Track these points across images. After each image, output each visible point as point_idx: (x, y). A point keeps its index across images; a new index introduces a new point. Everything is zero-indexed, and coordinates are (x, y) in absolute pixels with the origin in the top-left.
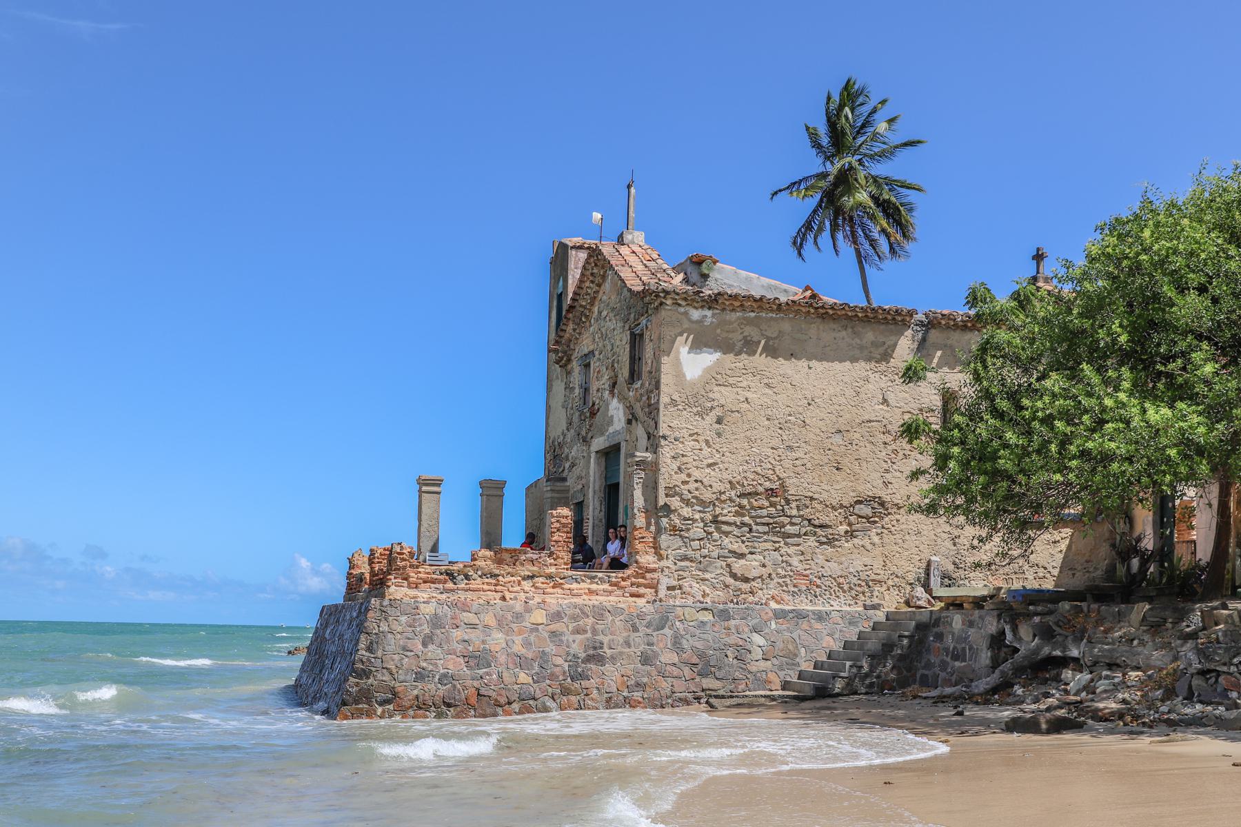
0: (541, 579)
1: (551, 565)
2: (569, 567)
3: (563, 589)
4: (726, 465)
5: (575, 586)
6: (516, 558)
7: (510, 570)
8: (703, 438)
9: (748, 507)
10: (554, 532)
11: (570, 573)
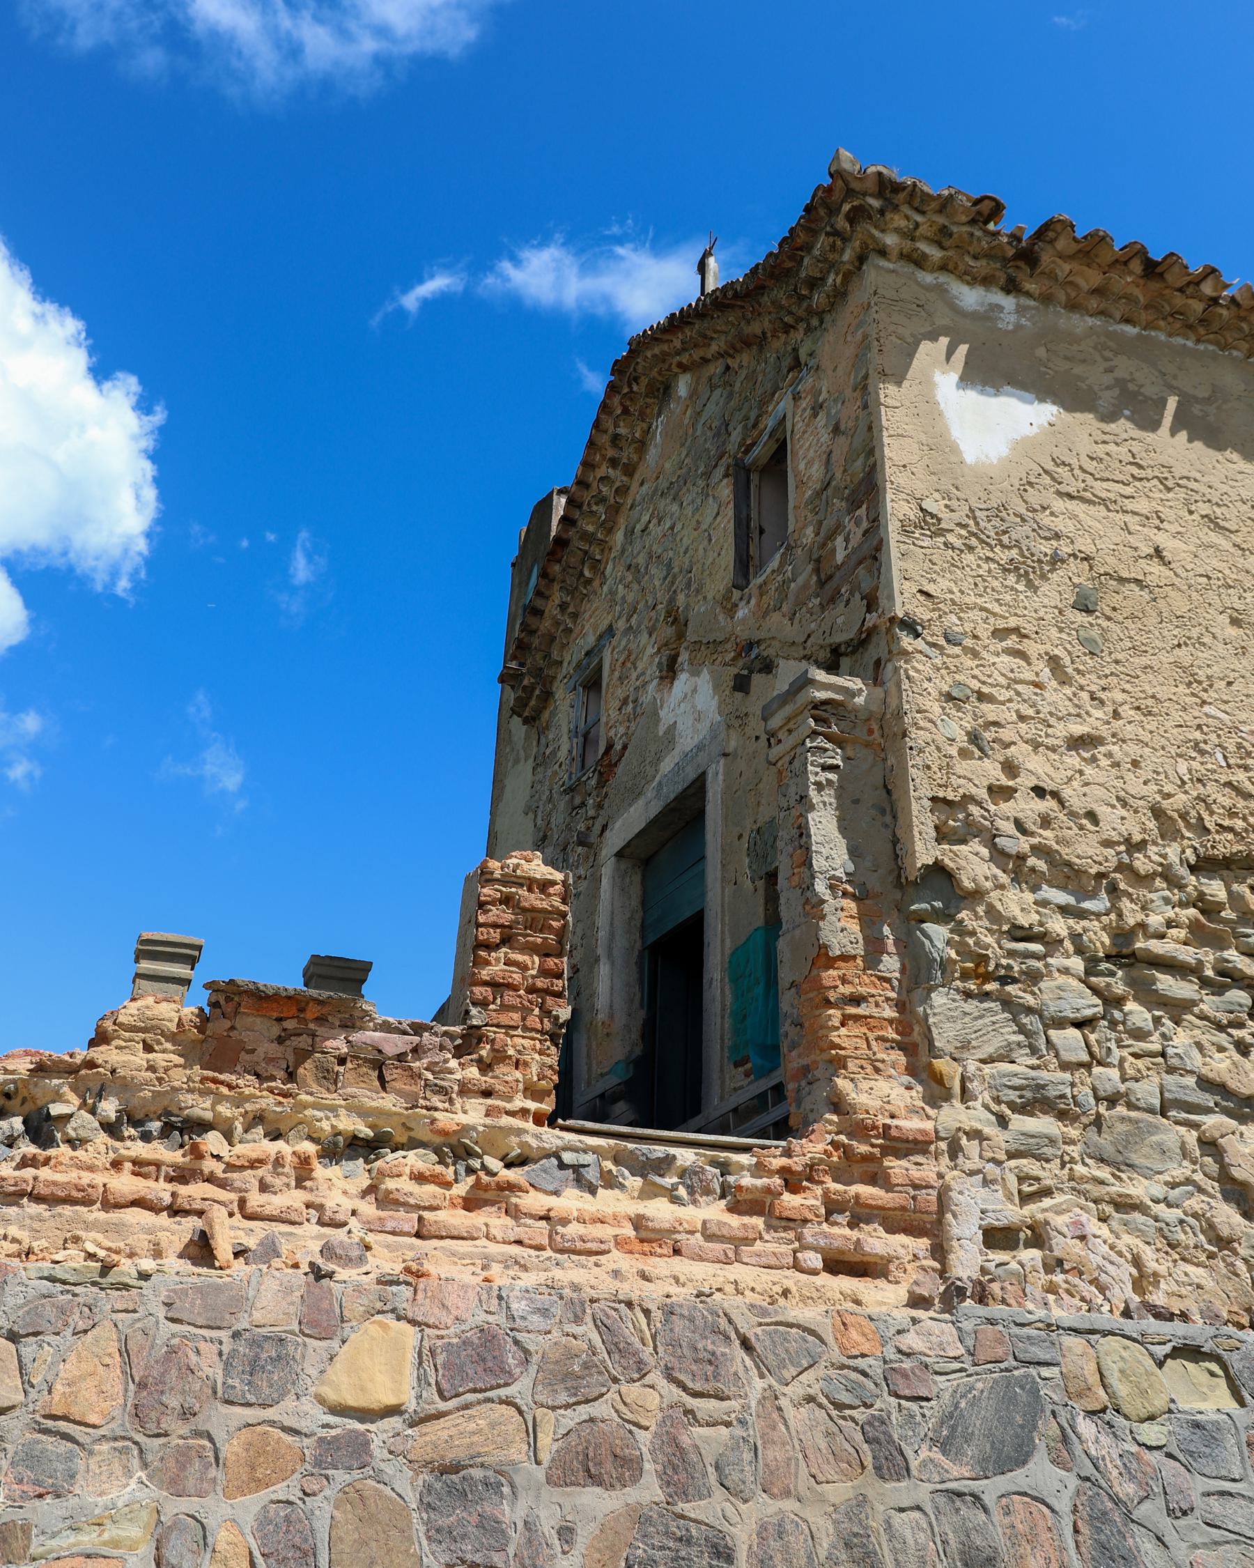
0: (416, 1160)
1: (465, 1090)
2: (547, 1106)
3: (514, 1213)
4: (1133, 750)
5: (571, 1201)
6: (303, 1042)
7: (268, 1102)
8: (1042, 649)
9: (1228, 914)
10: (489, 947)
11: (552, 1137)
